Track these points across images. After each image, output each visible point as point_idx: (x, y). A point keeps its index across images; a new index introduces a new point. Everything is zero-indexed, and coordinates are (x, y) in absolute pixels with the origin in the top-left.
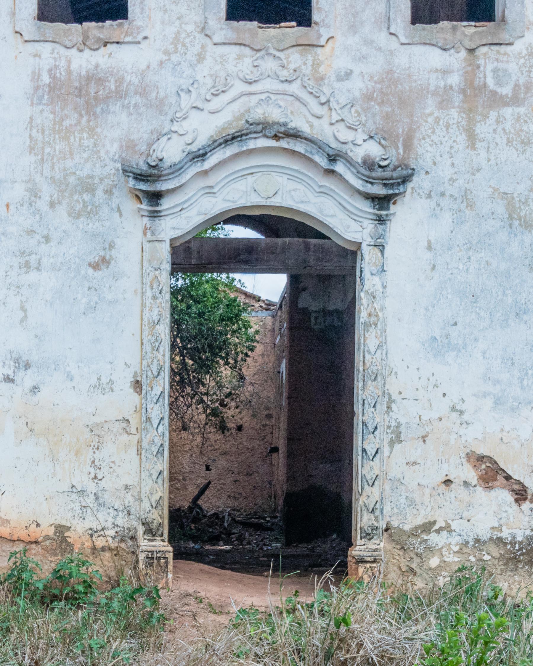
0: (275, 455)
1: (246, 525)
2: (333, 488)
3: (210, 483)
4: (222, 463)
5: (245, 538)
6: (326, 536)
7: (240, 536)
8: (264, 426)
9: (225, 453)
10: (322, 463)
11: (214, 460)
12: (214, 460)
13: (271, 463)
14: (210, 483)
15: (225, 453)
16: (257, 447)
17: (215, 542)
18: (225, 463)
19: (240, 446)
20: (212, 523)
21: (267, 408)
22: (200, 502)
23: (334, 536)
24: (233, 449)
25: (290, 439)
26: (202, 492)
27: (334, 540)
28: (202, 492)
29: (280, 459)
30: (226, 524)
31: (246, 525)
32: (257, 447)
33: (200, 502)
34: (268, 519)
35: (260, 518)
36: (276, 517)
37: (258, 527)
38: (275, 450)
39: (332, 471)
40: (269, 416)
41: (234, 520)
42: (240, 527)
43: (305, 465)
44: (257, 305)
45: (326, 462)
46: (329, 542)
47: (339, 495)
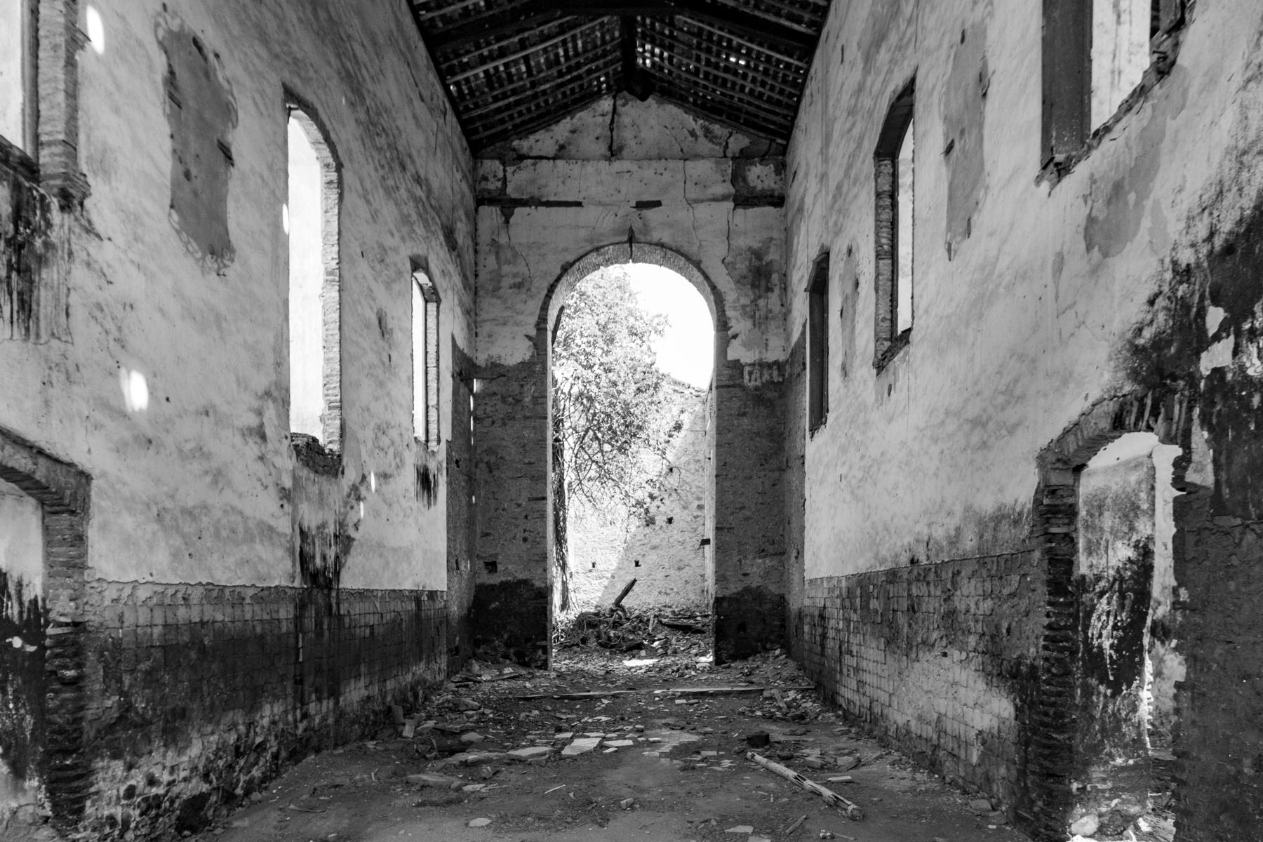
0: (707, 547)
1: (674, 627)
2: (773, 588)
3: (635, 581)
4: (652, 557)
5: (671, 645)
6: (767, 650)
7: (666, 642)
8: (696, 517)
9: (654, 548)
10: (760, 558)
11: (644, 555)
12: (644, 555)
13: (704, 556)
14: (635, 581)
15: (654, 548)
16: (688, 540)
17: (635, 652)
18: (655, 557)
19: (671, 540)
20: (635, 627)
21: (699, 499)
22: (623, 602)
23: (778, 652)
24: (664, 543)
25: (718, 529)
26: (626, 592)
27: (777, 657)
28: (626, 592)
29: (709, 550)
30: (650, 628)
31: (674, 627)
32: (688, 540)
33: (623, 602)
34: (699, 618)
35: (690, 617)
36: (707, 616)
37: (686, 629)
38: (705, 542)
39: (773, 566)
40: (700, 507)
41: (660, 622)
42: (666, 631)
43: (740, 561)
44: (687, 392)
45: (765, 556)
46: (771, 659)
47: (782, 597)
